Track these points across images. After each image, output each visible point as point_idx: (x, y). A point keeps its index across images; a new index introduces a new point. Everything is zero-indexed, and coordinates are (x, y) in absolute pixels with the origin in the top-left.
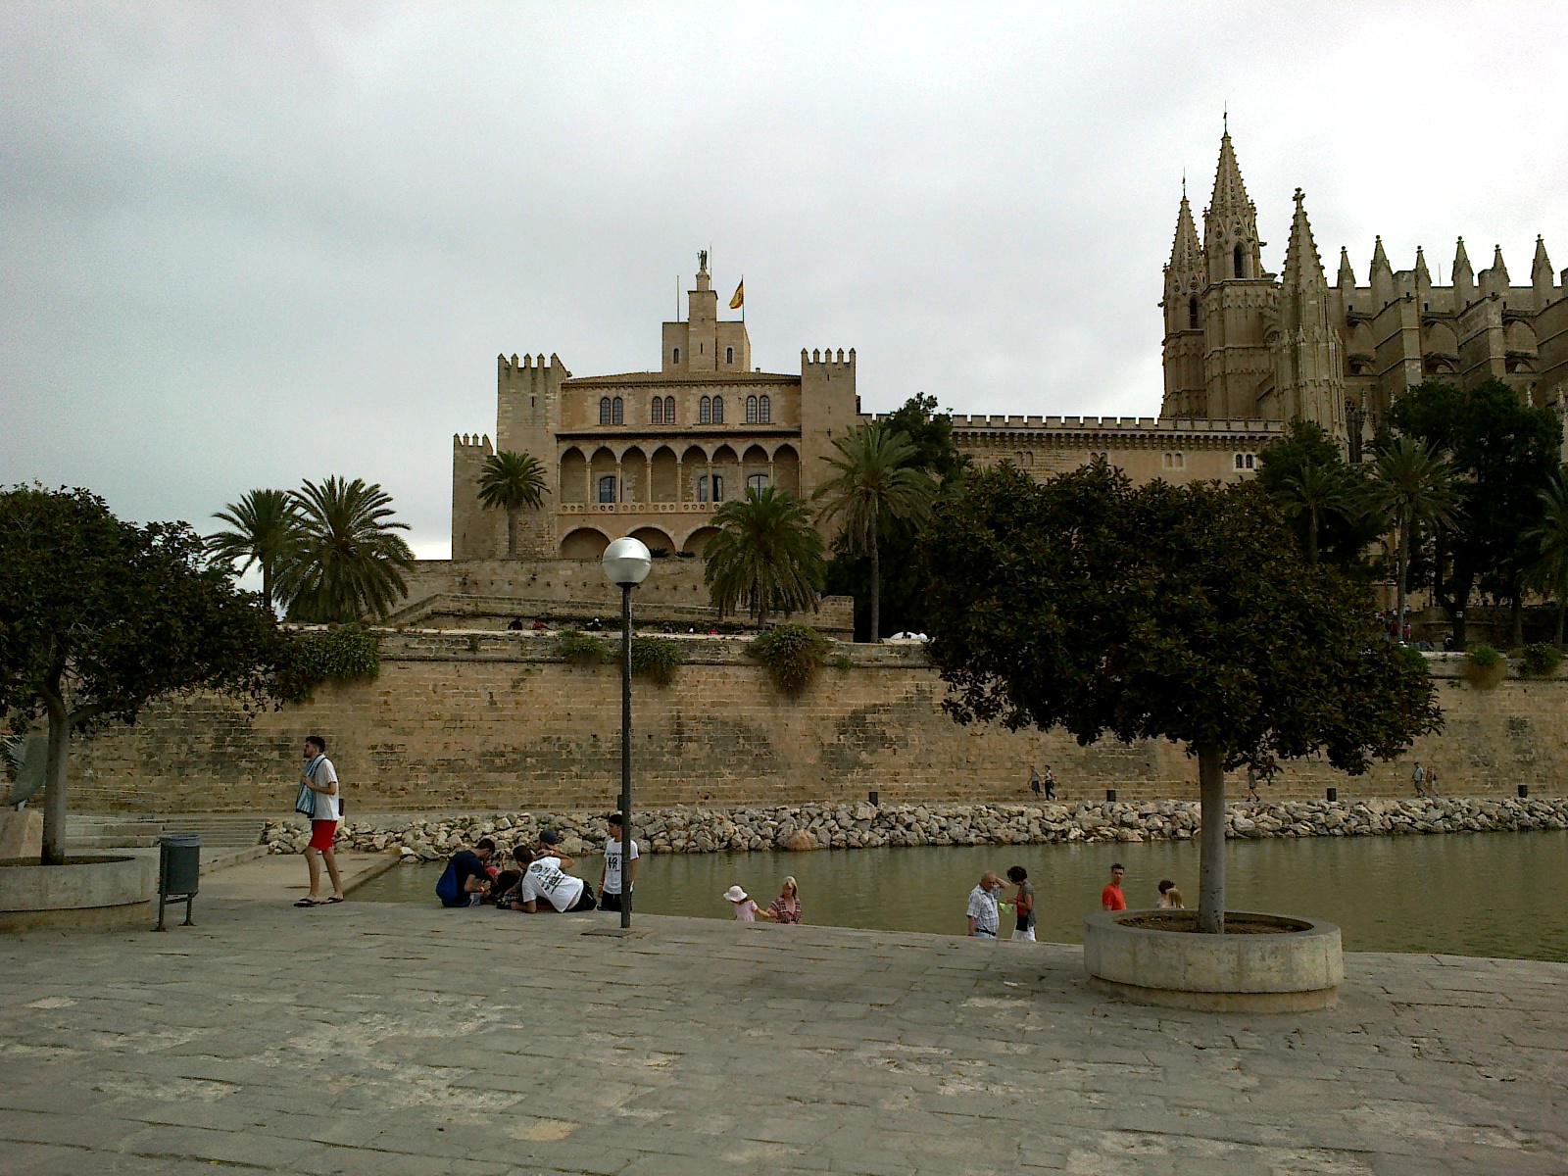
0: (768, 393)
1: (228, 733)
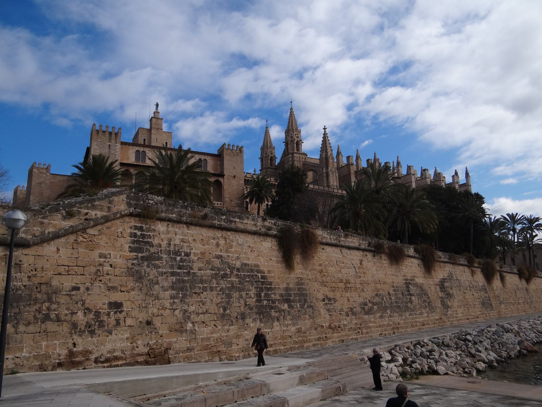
0: (207, 158)
1: (261, 290)
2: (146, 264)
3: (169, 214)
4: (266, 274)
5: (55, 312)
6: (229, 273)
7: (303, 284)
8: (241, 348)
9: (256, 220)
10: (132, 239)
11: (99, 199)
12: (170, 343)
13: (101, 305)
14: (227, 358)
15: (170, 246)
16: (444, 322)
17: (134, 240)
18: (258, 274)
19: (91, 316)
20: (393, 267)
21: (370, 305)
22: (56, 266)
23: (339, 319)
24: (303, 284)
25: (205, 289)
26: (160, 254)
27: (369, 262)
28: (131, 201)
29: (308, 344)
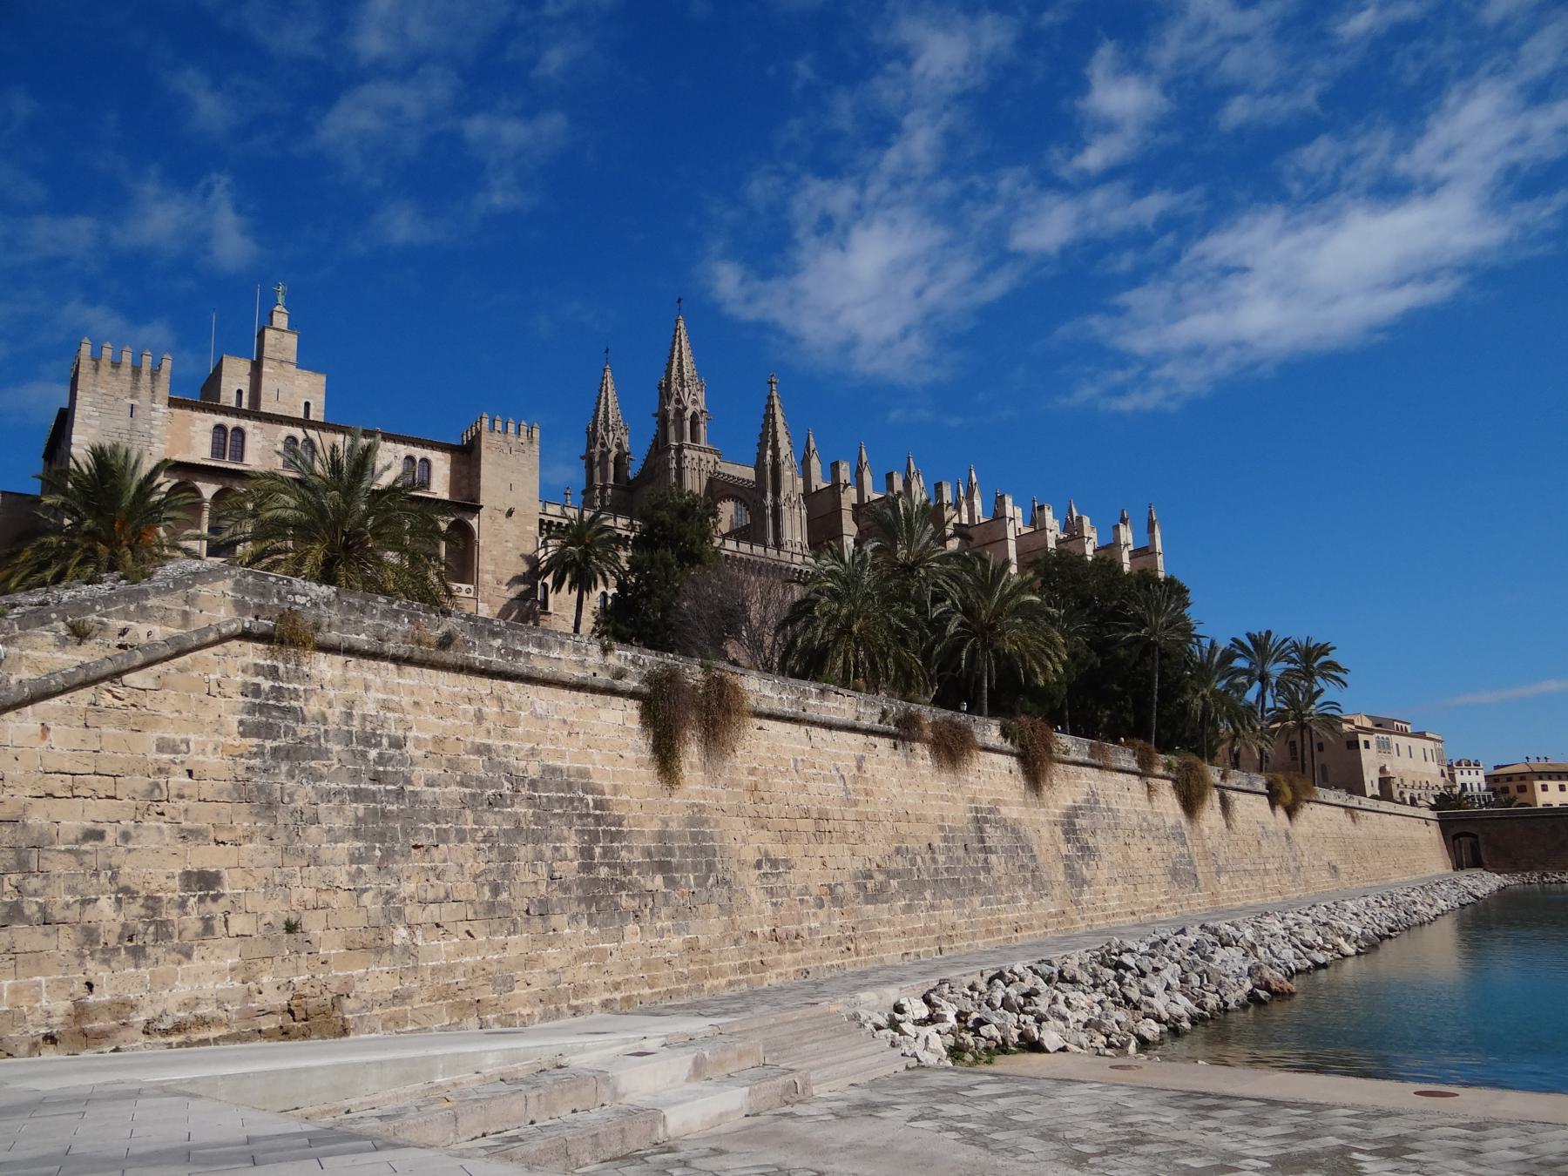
1: (595, 837)
2: (284, 767)
3: (348, 632)
4: (608, 797)
5: (38, 899)
6: (508, 792)
7: (705, 822)
8: (536, 992)
9: (584, 651)
10: (247, 700)
11: (158, 591)
12: (347, 982)
13: (163, 880)
14: (498, 1020)
15: (352, 720)
16: (1072, 921)
17: (254, 704)
18: (586, 796)
19: (136, 909)
20: (944, 775)
21: (880, 877)
22: (40, 775)
23: (799, 914)
24: (705, 822)
25: (443, 836)
26: (322, 740)
27: (881, 763)
28: (247, 598)
29: (716, 982)
